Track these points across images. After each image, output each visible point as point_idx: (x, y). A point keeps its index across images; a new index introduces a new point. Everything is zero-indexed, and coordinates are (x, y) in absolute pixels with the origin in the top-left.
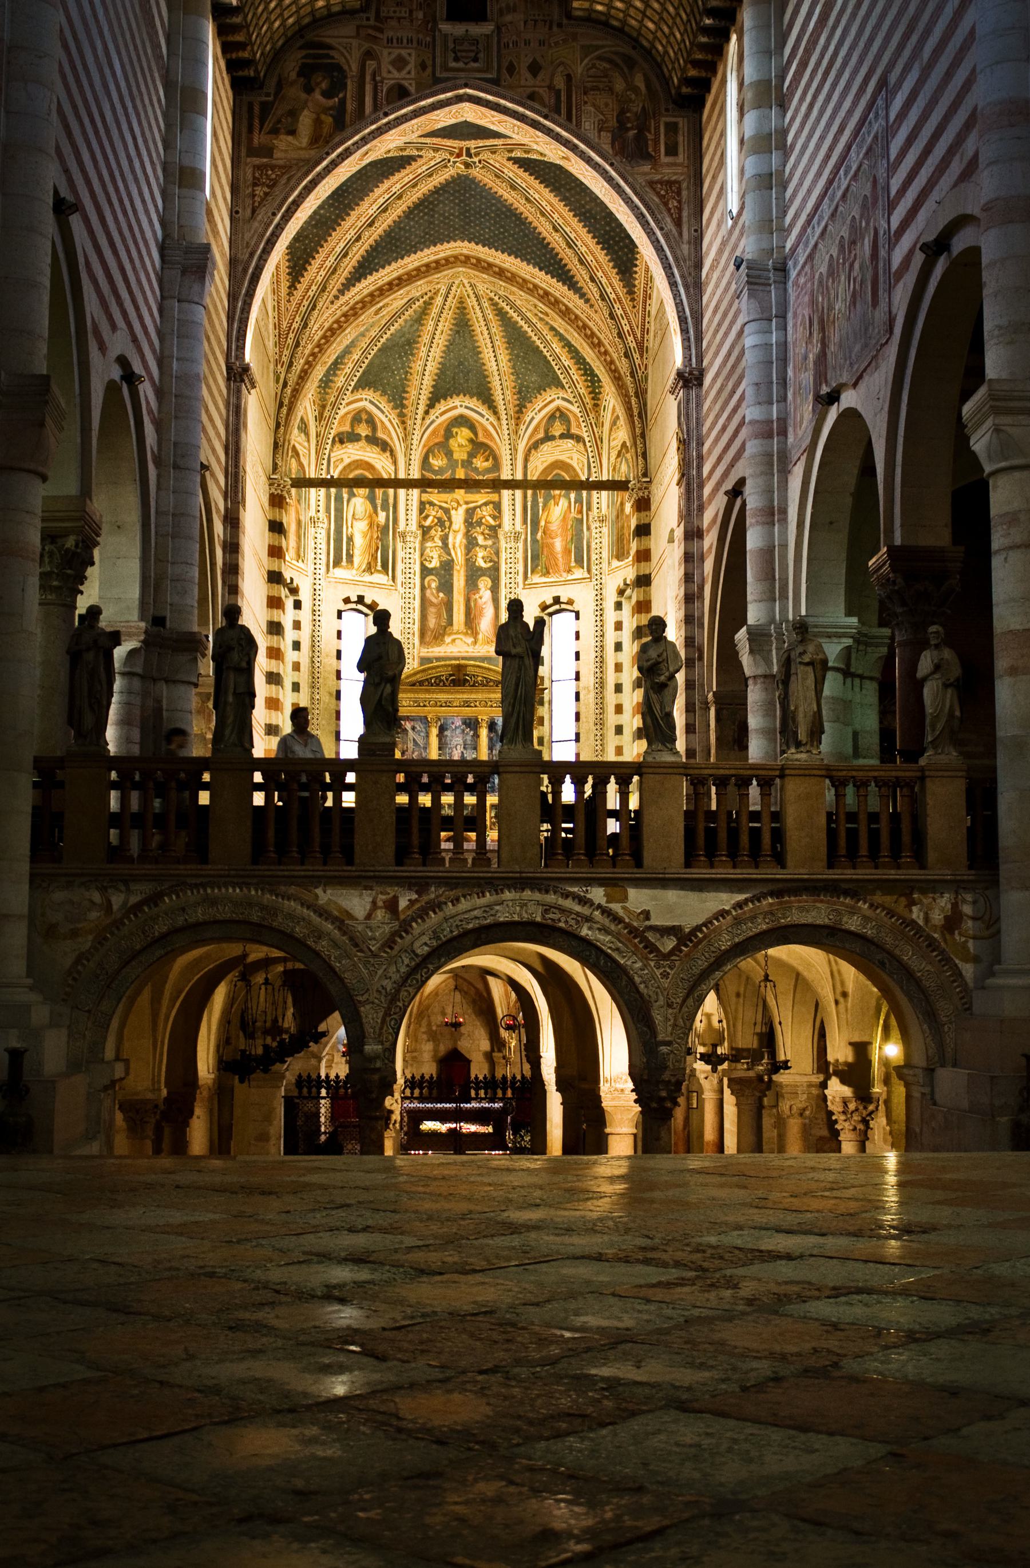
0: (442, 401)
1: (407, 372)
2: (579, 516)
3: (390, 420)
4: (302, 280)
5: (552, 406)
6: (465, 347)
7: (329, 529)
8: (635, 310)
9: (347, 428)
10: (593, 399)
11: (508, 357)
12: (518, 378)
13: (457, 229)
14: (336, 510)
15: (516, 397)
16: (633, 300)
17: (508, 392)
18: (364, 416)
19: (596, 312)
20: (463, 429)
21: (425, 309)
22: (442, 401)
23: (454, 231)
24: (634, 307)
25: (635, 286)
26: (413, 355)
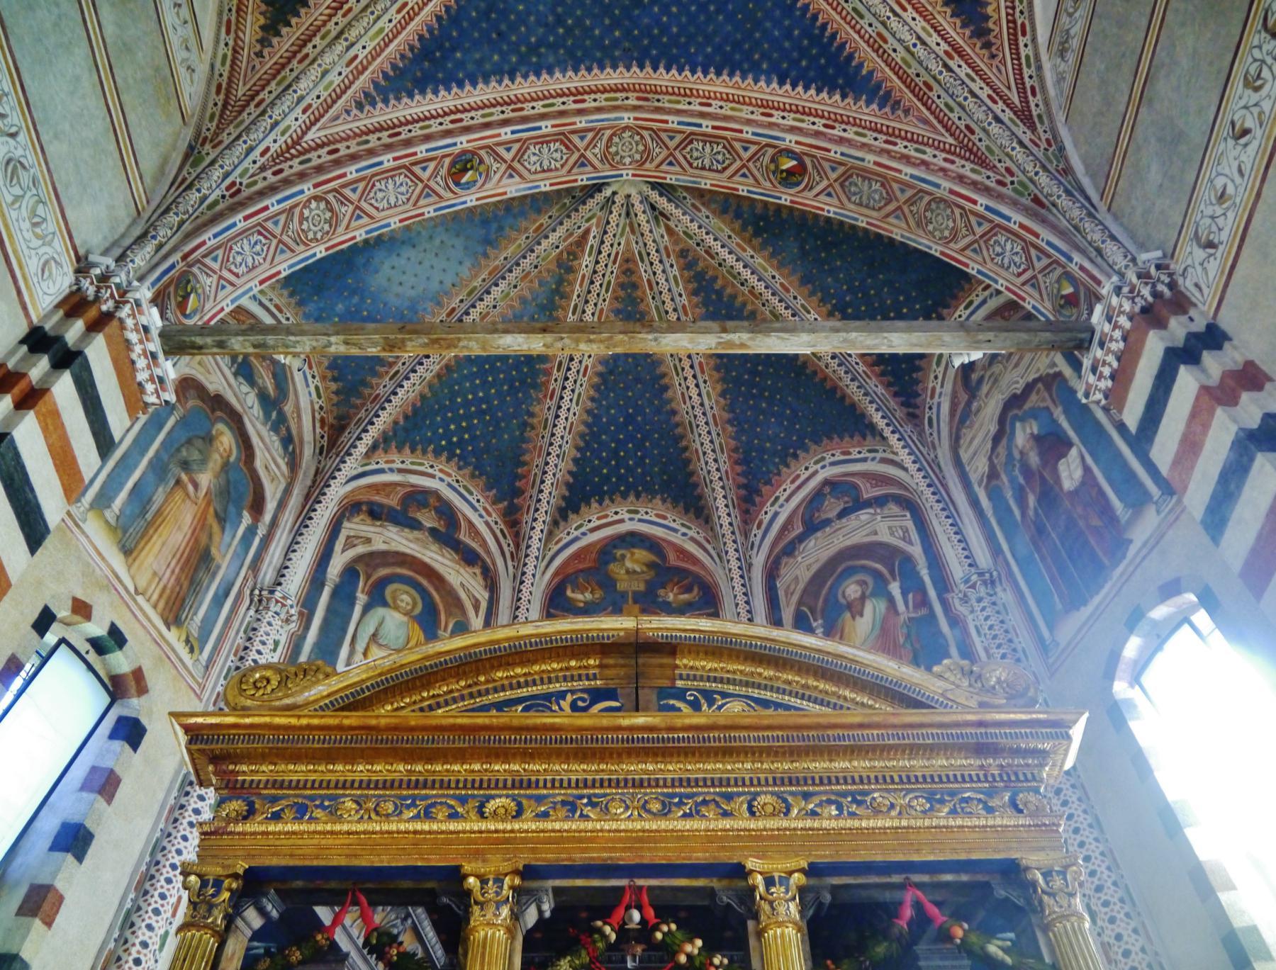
0: (595, 505)
1: (525, 424)
2: (924, 612)
3: (487, 523)
4: (294, 21)
5: (813, 484)
6: (637, 380)
7: (303, 638)
8: (996, 62)
9: (393, 501)
10: (903, 404)
11: (719, 387)
12: (741, 431)
13: (616, 24)
14: (330, 610)
15: (739, 469)
16: (987, 45)
17: (723, 458)
18: (432, 501)
19: (907, 112)
20: (636, 551)
21: (560, 282)
22: (595, 505)
23: (610, 29)
24: (993, 56)
25: (987, 18)
26: (535, 386)
